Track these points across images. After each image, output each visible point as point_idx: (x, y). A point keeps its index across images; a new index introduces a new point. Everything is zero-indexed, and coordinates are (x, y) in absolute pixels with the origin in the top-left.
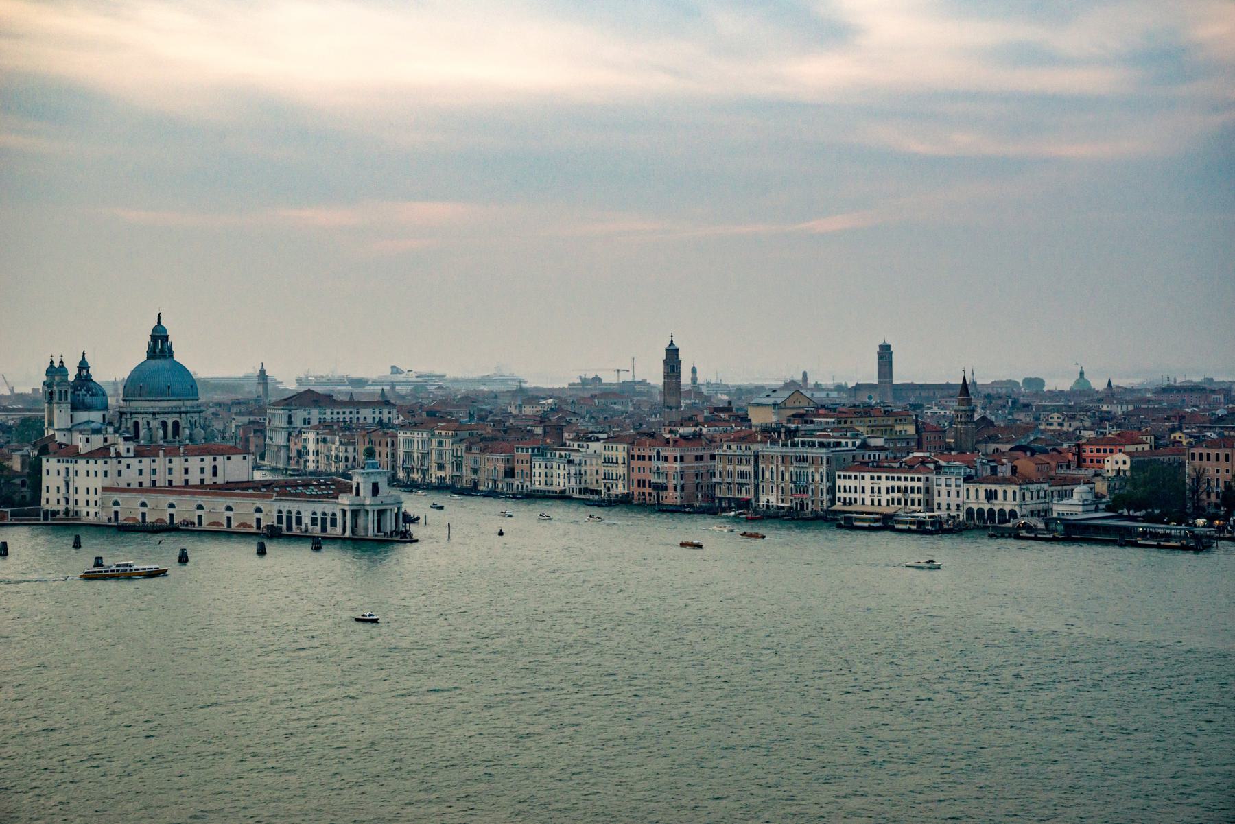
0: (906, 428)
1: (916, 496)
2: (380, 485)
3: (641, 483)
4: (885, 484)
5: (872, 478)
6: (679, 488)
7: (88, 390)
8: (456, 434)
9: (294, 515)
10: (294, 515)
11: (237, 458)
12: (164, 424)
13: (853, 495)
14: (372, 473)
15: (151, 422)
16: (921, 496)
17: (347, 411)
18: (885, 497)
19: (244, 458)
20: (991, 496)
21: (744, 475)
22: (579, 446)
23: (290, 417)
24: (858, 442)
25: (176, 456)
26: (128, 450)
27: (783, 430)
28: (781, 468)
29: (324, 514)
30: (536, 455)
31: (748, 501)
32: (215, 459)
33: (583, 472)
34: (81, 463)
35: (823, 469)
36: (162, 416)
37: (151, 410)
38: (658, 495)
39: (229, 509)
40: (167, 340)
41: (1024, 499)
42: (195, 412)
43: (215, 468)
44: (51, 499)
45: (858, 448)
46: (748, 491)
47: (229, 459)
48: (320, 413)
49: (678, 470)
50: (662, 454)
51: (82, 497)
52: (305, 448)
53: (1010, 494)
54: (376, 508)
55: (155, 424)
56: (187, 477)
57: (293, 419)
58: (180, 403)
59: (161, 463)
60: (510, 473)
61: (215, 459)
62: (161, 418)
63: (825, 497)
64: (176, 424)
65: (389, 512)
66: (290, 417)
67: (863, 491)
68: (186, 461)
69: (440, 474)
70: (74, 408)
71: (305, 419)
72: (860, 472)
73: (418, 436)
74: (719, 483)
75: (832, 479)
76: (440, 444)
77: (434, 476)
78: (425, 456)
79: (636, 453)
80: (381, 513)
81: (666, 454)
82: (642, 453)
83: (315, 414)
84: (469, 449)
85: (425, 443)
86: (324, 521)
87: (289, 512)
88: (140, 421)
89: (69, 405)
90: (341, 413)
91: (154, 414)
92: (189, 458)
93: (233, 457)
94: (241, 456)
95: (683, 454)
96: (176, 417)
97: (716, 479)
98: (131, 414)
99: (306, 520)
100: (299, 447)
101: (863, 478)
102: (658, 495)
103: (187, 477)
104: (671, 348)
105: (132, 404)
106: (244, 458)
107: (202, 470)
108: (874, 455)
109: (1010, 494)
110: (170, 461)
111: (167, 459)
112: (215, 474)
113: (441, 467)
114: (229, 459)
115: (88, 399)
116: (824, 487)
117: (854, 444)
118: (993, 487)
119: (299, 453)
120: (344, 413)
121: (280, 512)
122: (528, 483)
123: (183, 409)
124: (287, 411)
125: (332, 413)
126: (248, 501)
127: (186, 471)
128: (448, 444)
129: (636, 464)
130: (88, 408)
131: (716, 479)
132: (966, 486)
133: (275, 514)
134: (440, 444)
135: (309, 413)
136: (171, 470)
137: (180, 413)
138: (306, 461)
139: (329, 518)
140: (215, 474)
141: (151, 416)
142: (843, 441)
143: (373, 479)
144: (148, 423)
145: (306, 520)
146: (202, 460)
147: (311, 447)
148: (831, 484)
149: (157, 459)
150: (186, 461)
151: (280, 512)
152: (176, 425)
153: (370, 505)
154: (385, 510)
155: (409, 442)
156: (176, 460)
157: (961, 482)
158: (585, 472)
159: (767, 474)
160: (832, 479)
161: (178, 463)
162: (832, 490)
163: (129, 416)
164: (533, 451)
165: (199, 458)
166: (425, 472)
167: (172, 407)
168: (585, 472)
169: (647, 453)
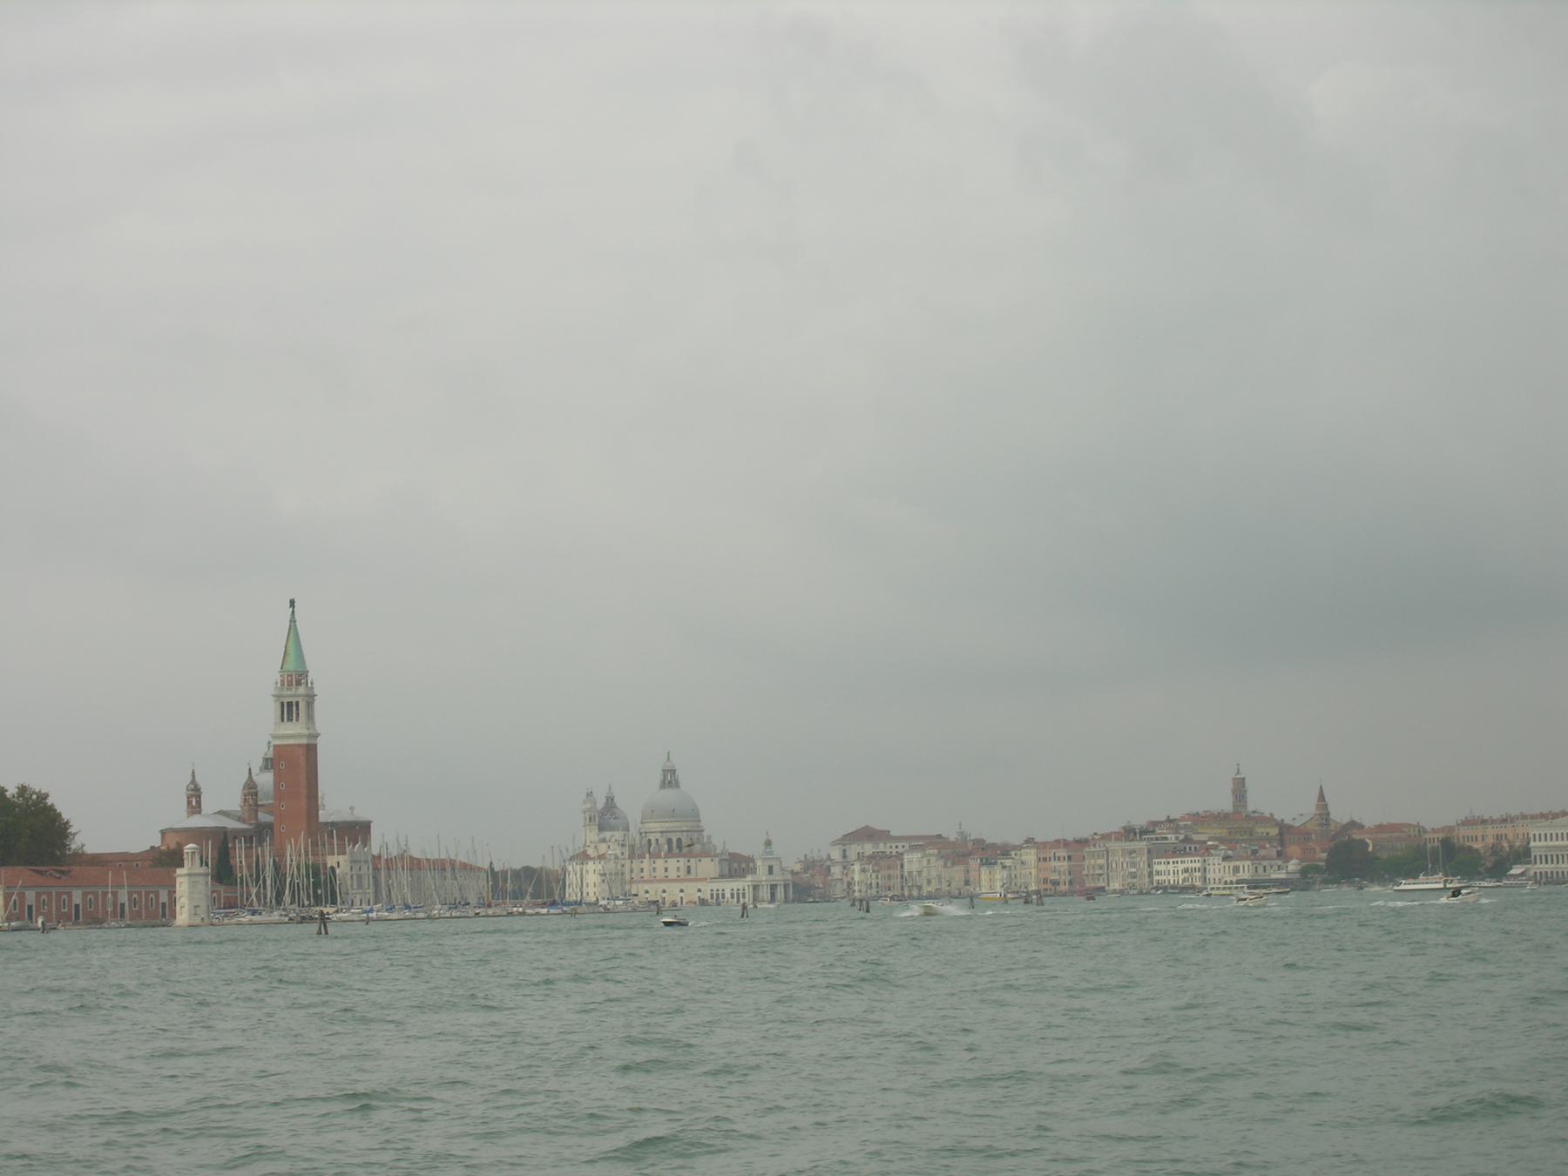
0: (1268, 830)
1: (1197, 874)
2: (774, 868)
3: (1045, 881)
4: (1181, 867)
5: (1174, 863)
6: (1067, 883)
7: (611, 815)
8: (939, 852)
9: (720, 892)
10: (720, 892)
11: (706, 861)
12: (669, 841)
13: (1164, 878)
14: (768, 859)
15: (660, 839)
16: (1200, 874)
17: (900, 845)
18: (1181, 877)
19: (712, 860)
20: (1236, 869)
21: (1101, 867)
22: (1015, 854)
23: (844, 850)
24: (1182, 837)
25: (657, 858)
26: (622, 854)
27: (1137, 831)
28: (1121, 860)
29: (738, 890)
30: (984, 864)
31: (1104, 887)
32: (689, 861)
33: (1013, 876)
34: (591, 863)
35: (1145, 858)
36: (669, 834)
37: (660, 829)
38: (1055, 889)
39: (682, 891)
40: (674, 773)
41: (1256, 871)
42: (695, 831)
43: (689, 867)
44: (571, 894)
45: (1182, 841)
46: (1103, 881)
47: (700, 861)
48: (873, 847)
49: (1066, 867)
50: (1057, 855)
51: (591, 890)
52: (853, 879)
53: (1246, 868)
54: (769, 883)
55: (662, 841)
56: (667, 874)
57: (848, 853)
58: (683, 823)
59: (646, 863)
60: (967, 883)
61: (689, 861)
62: (670, 835)
63: (1147, 880)
64: (679, 840)
65: (779, 887)
66: (844, 850)
67: (1169, 874)
68: (666, 862)
69: (930, 889)
70: (601, 828)
71: (859, 853)
72: (1167, 858)
73: (916, 856)
74: (1087, 875)
75: (1150, 866)
76: (929, 861)
77: (926, 889)
78: (920, 873)
79: (1041, 856)
80: (773, 887)
81: (1060, 854)
82: (1045, 856)
83: (868, 849)
84: (945, 866)
85: (920, 861)
86: (738, 894)
87: (718, 890)
88: (651, 838)
89: (597, 827)
90: (894, 847)
91: (662, 832)
92: (669, 860)
93: (703, 860)
94: (710, 859)
95: (1070, 854)
96: (679, 835)
97: (1085, 872)
98: (646, 833)
99: (728, 895)
100: (849, 879)
101: (1168, 863)
102: (1055, 889)
103: (667, 874)
104: (1238, 776)
105: (647, 825)
106: (712, 860)
107: (678, 868)
108: (1190, 848)
109: (1246, 868)
110: (654, 862)
111: (652, 860)
112: (689, 872)
113: (929, 882)
114: (700, 861)
115: (612, 821)
116: (1146, 873)
117: (1177, 838)
118: (1237, 863)
119: (849, 884)
120: (897, 847)
121: (712, 890)
122: (978, 889)
123: (684, 829)
124: (841, 846)
125: (885, 847)
126: (693, 884)
127: (666, 870)
128: (933, 859)
129: (1042, 864)
130: (612, 829)
131: (1085, 872)
132: (1223, 864)
133: (709, 892)
134: (929, 861)
135: (863, 848)
136: (654, 869)
137: (683, 831)
138: (854, 891)
139: (741, 892)
140: (689, 872)
141: (659, 834)
142: (1169, 836)
143: (769, 863)
144: (657, 840)
145: (728, 895)
146: (678, 861)
147: (857, 878)
148: (1245, 886)
149: (644, 860)
150: (666, 862)
151: (712, 890)
152: (679, 840)
153: (765, 881)
154: (776, 885)
155: (910, 861)
156: (658, 861)
157: (1220, 861)
158: (1016, 876)
159: (1114, 866)
160: (1150, 866)
161: (660, 863)
162: (1150, 874)
163: (644, 835)
164: (981, 860)
165: (676, 860)
166: (920, 888)
167: (677, 827)
168: (1016, 876)
169: (1047, 856)
